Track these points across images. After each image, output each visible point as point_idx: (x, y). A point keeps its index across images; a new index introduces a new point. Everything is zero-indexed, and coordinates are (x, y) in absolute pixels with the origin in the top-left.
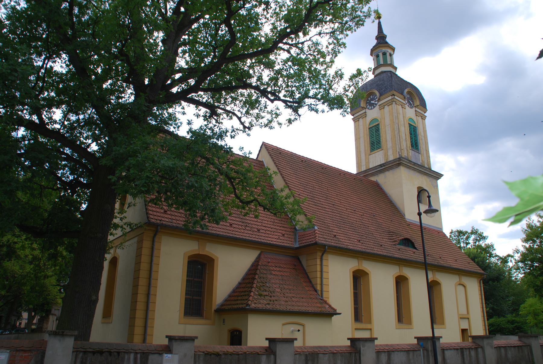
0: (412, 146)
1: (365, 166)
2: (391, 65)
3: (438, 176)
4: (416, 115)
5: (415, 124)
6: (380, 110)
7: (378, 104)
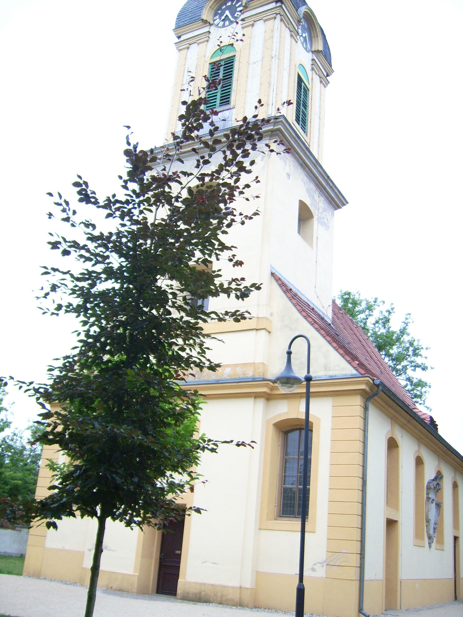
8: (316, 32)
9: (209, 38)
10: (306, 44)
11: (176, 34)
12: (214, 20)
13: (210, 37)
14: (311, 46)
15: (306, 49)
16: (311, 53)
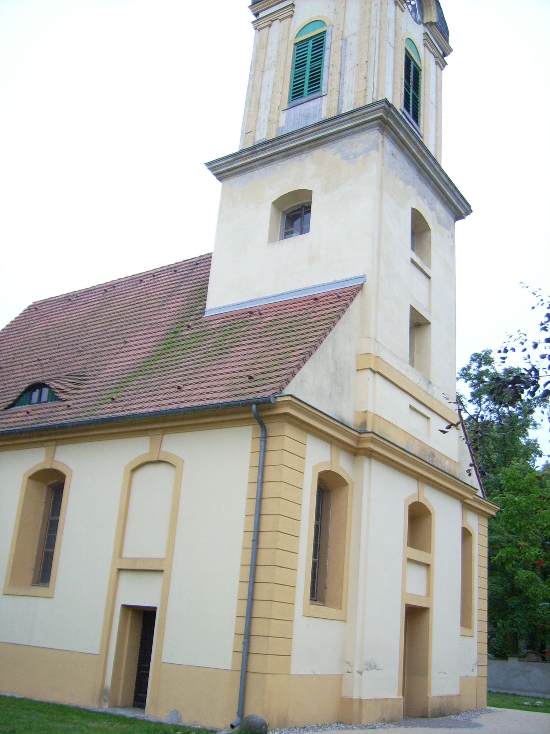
1: (265, 131)
9: (294, 12)
10: (416, 14)
11: (252, 11)
13: (294, 10)
14: (422, 18)
15: (415, 20)
16: (422, 25)
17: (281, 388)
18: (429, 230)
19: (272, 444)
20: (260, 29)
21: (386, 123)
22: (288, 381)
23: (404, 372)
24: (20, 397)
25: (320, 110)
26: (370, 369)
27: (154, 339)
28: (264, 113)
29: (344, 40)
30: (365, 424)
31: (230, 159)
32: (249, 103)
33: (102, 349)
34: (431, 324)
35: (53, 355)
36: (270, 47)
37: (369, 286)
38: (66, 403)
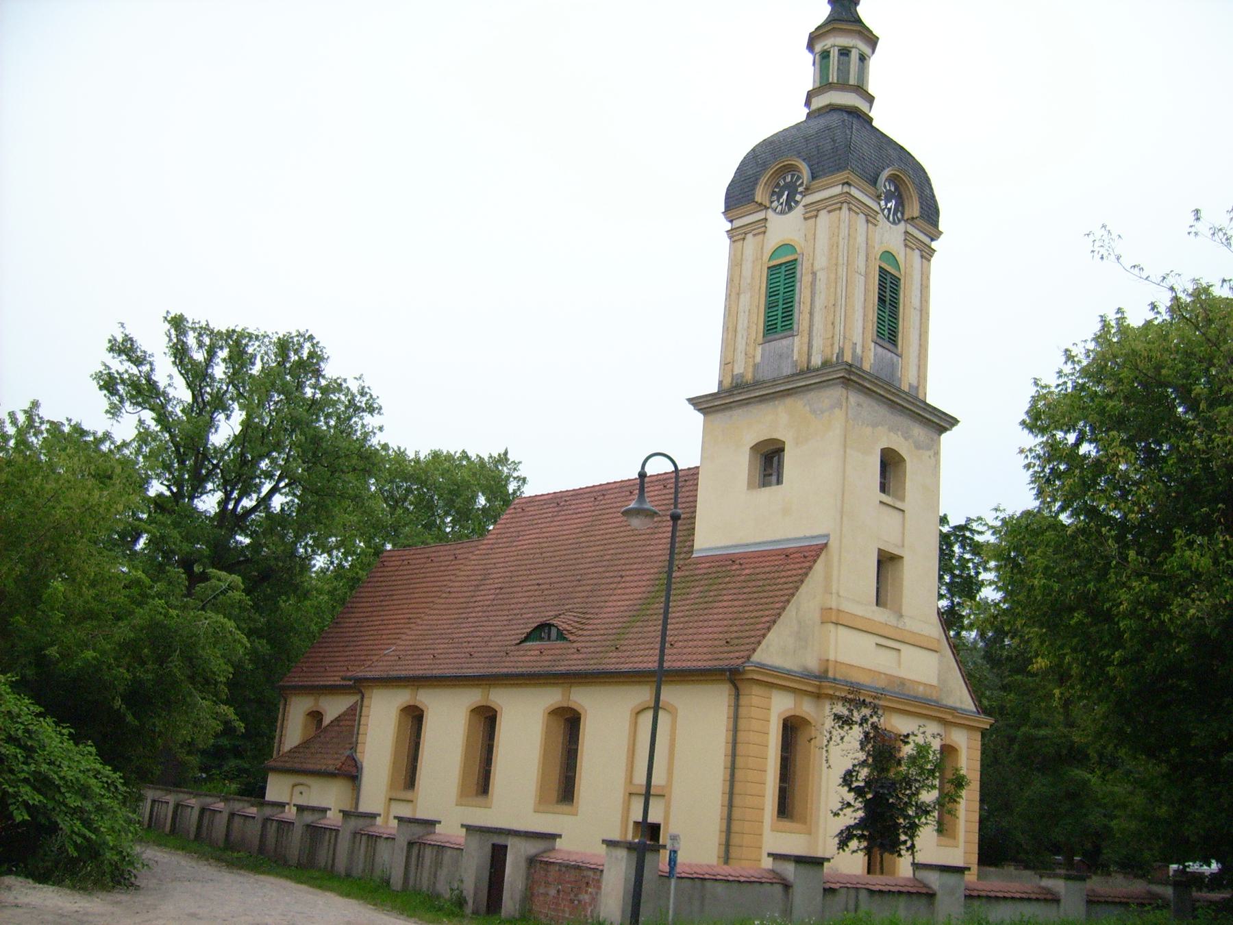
0: (880, 334)
2: (861, 90)
3: (941, 422)
4: (906, 246)
5: (899, 270)
6: (806, 219)
7: (803, 203)
8: (910, 192)
12: (772, 202)
17: (749, 657)
18: (904, 460)
19: (744, 700)
20: (734, 242)
21: (849, 380)
22: (754, 650)
23: (869, 615)
24: (531, 632)
25: (793, 350)
26: (833, 623)
27: (648, 577)
28: (741, 345)
29: (814, 274)
30: (826, 671)
31: (710, 398)
32: (726, 329)
33: (600, 581)
34: (905, 559)
35: (553, 580)
36: (744, 267)
37: (833, 544)
38: (575, 645)
